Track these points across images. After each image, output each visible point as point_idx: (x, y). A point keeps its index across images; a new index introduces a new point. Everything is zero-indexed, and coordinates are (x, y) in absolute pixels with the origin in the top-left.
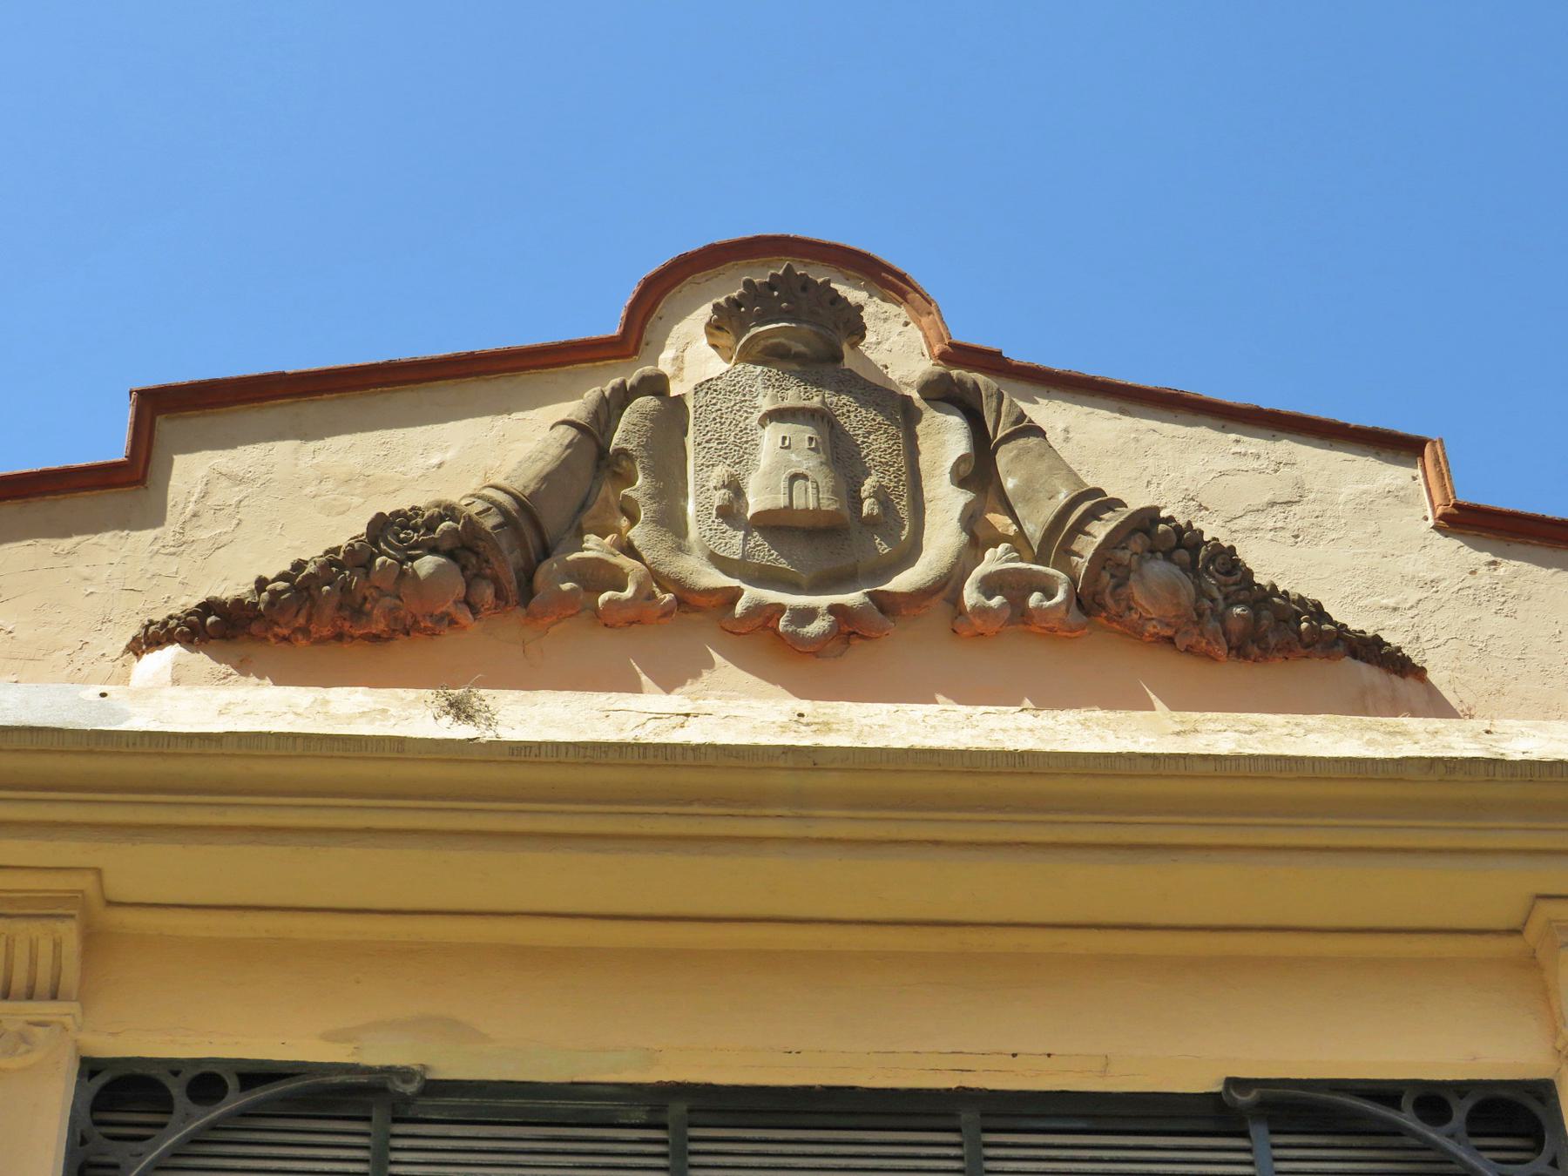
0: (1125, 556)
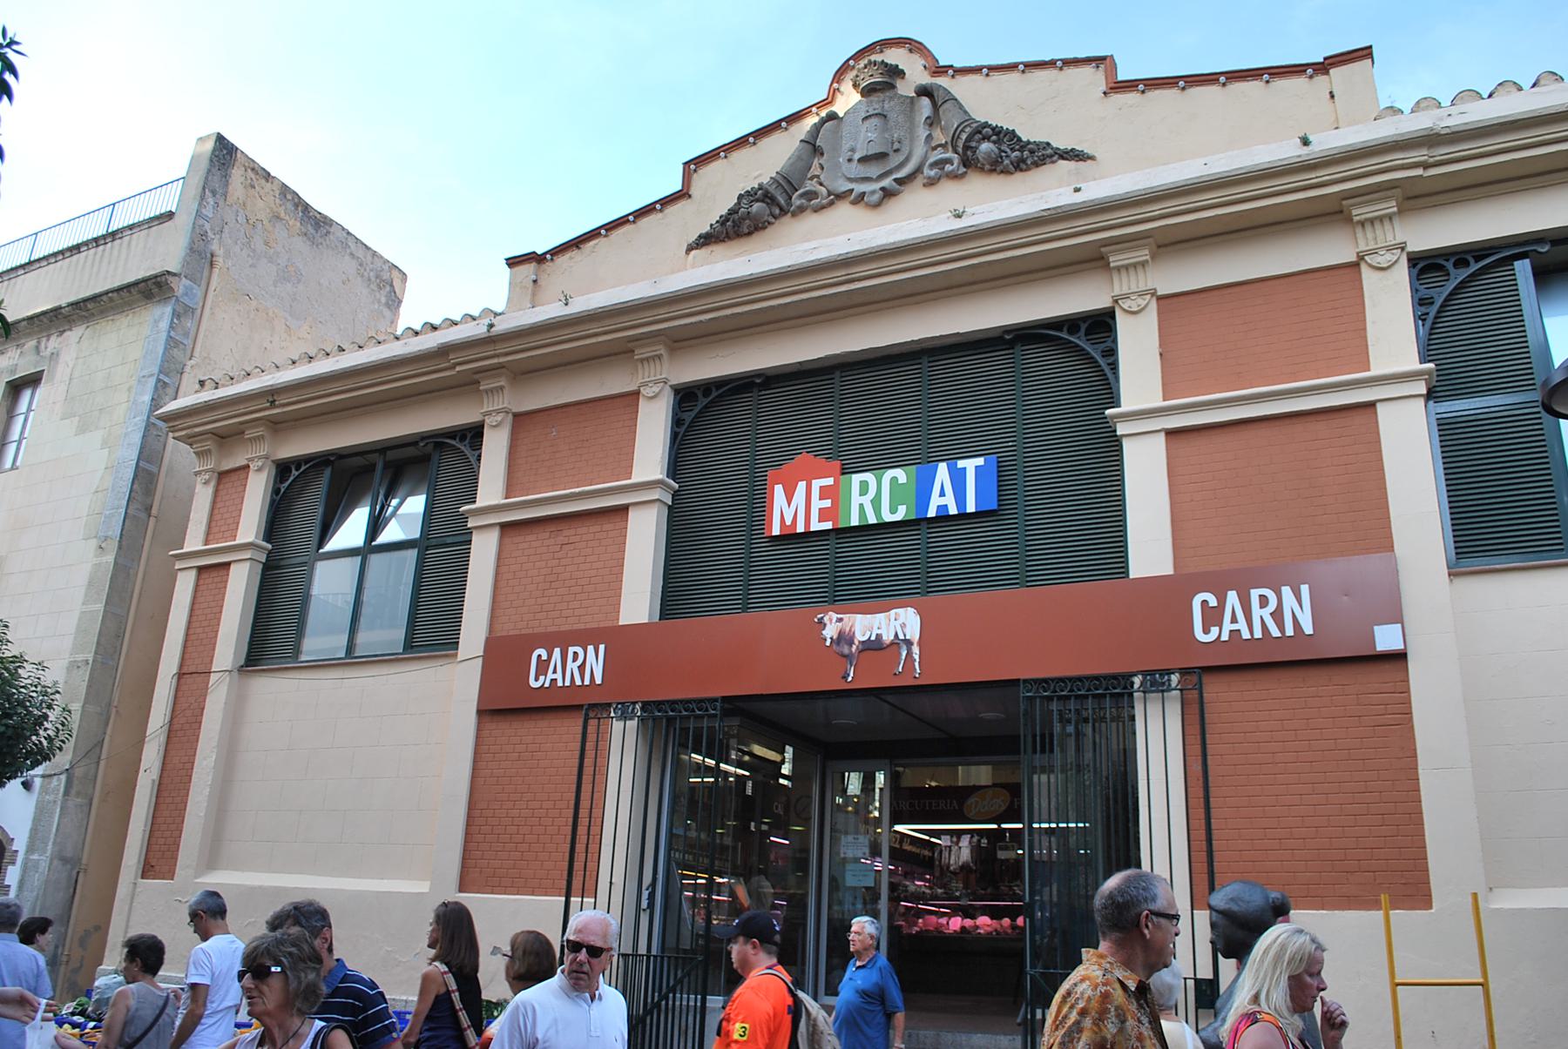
0: (973, 144)
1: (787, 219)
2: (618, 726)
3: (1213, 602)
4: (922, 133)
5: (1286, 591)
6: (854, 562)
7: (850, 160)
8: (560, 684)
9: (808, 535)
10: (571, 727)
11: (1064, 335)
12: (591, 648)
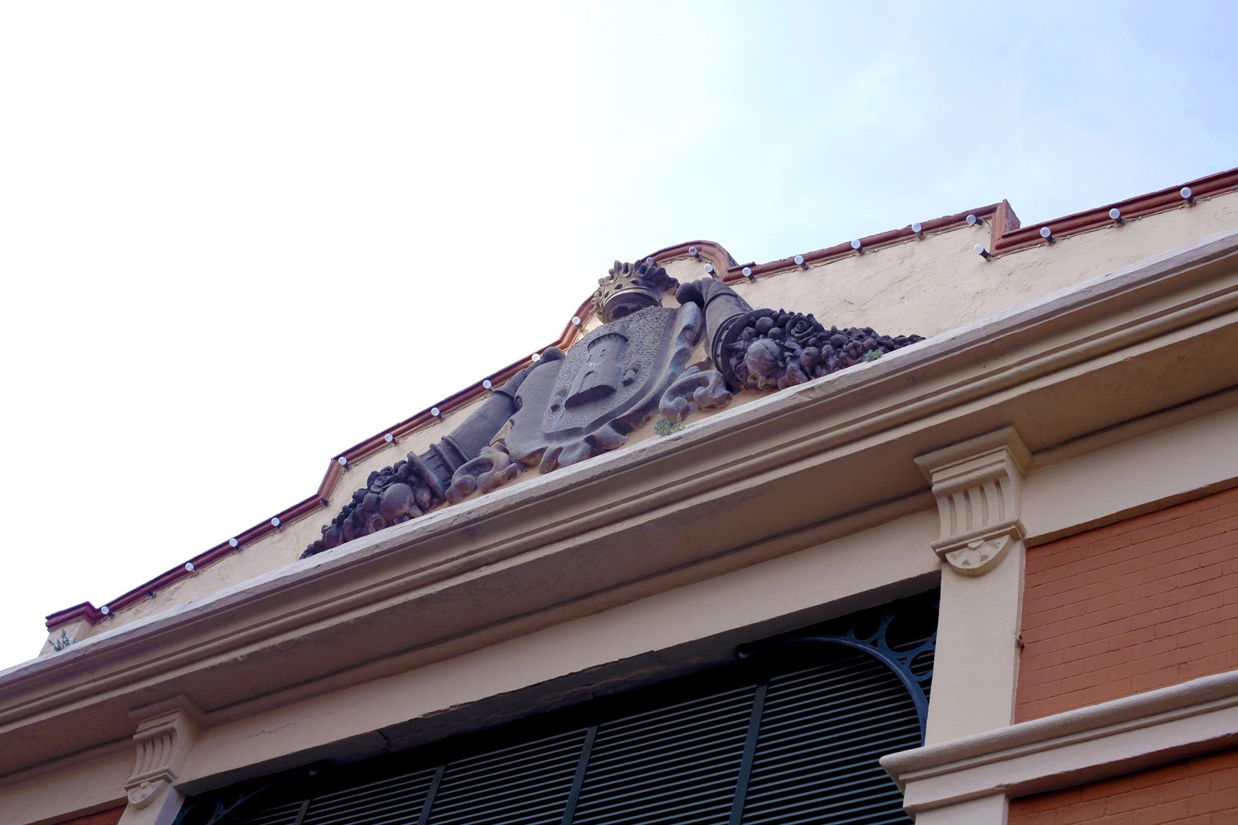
0: (740, 344)
11: (849, 640)
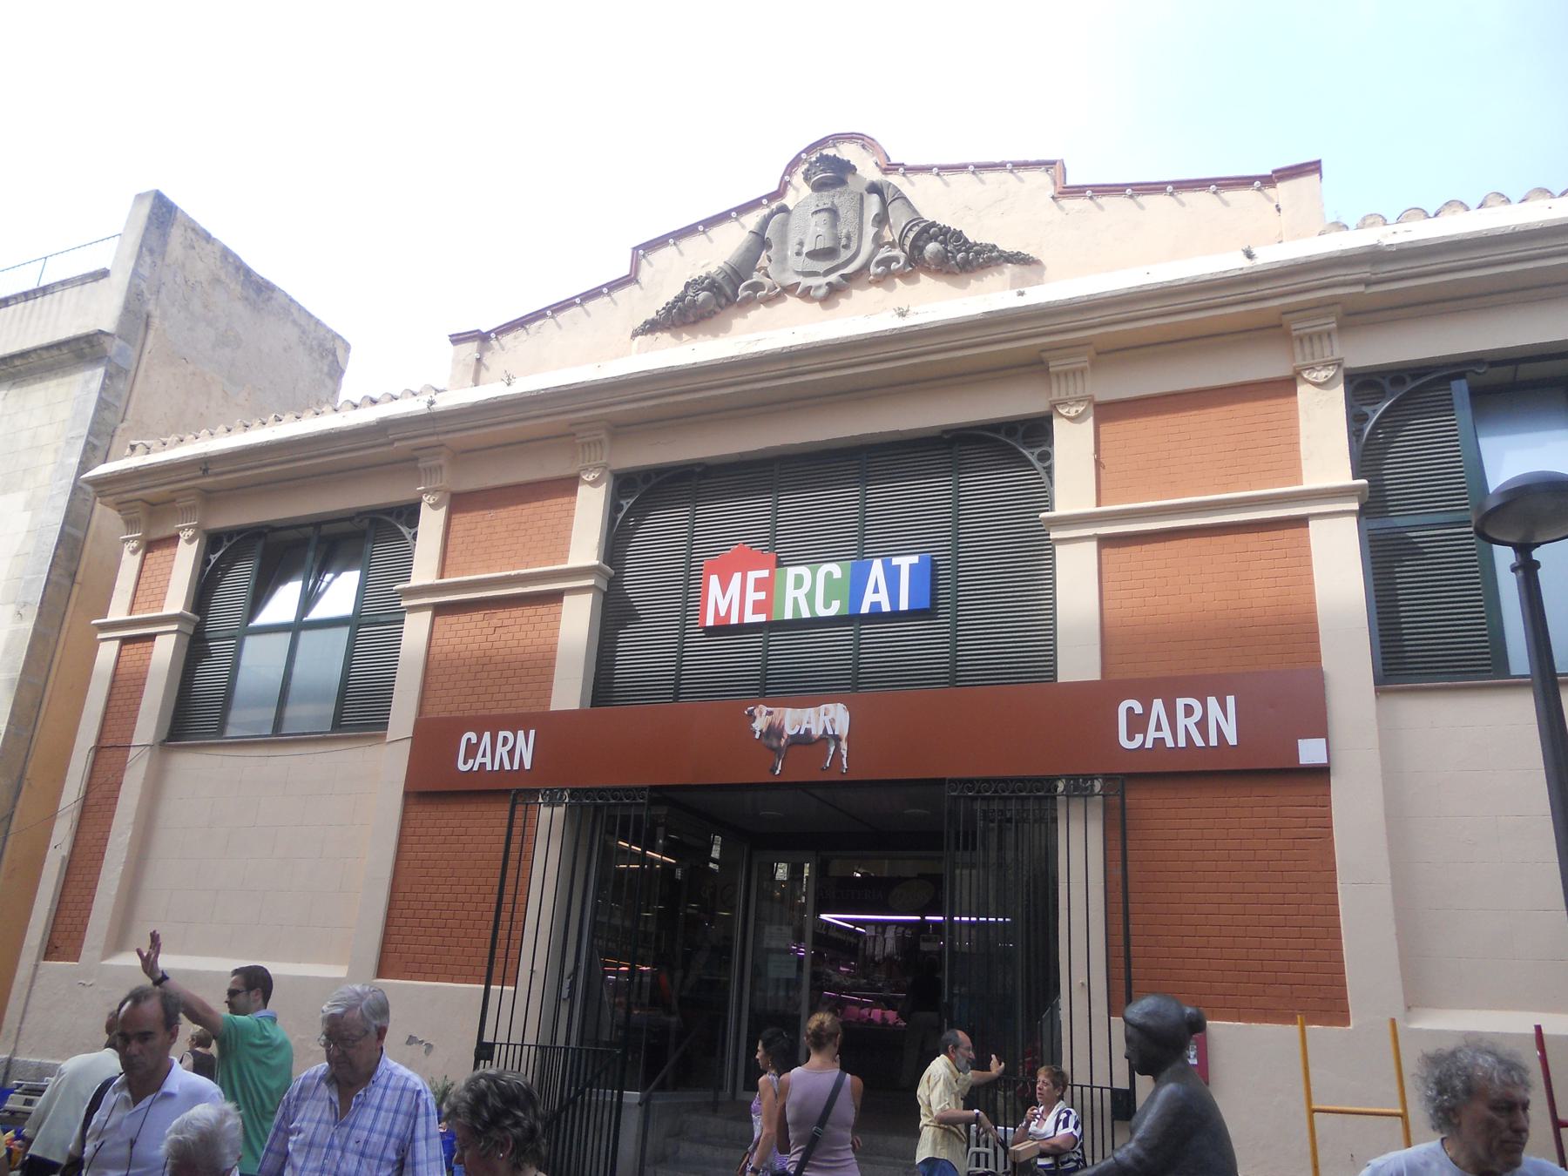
1: (732, 309)
2: (545, 812)
3: (1139, 709)
4: (870, 231)
5: (1212, 701)
6: (781, 658)
7: (798, 254)
8: (489, 768)
9: (743, 628)
10: (497, 814)
12: (521, 733)
